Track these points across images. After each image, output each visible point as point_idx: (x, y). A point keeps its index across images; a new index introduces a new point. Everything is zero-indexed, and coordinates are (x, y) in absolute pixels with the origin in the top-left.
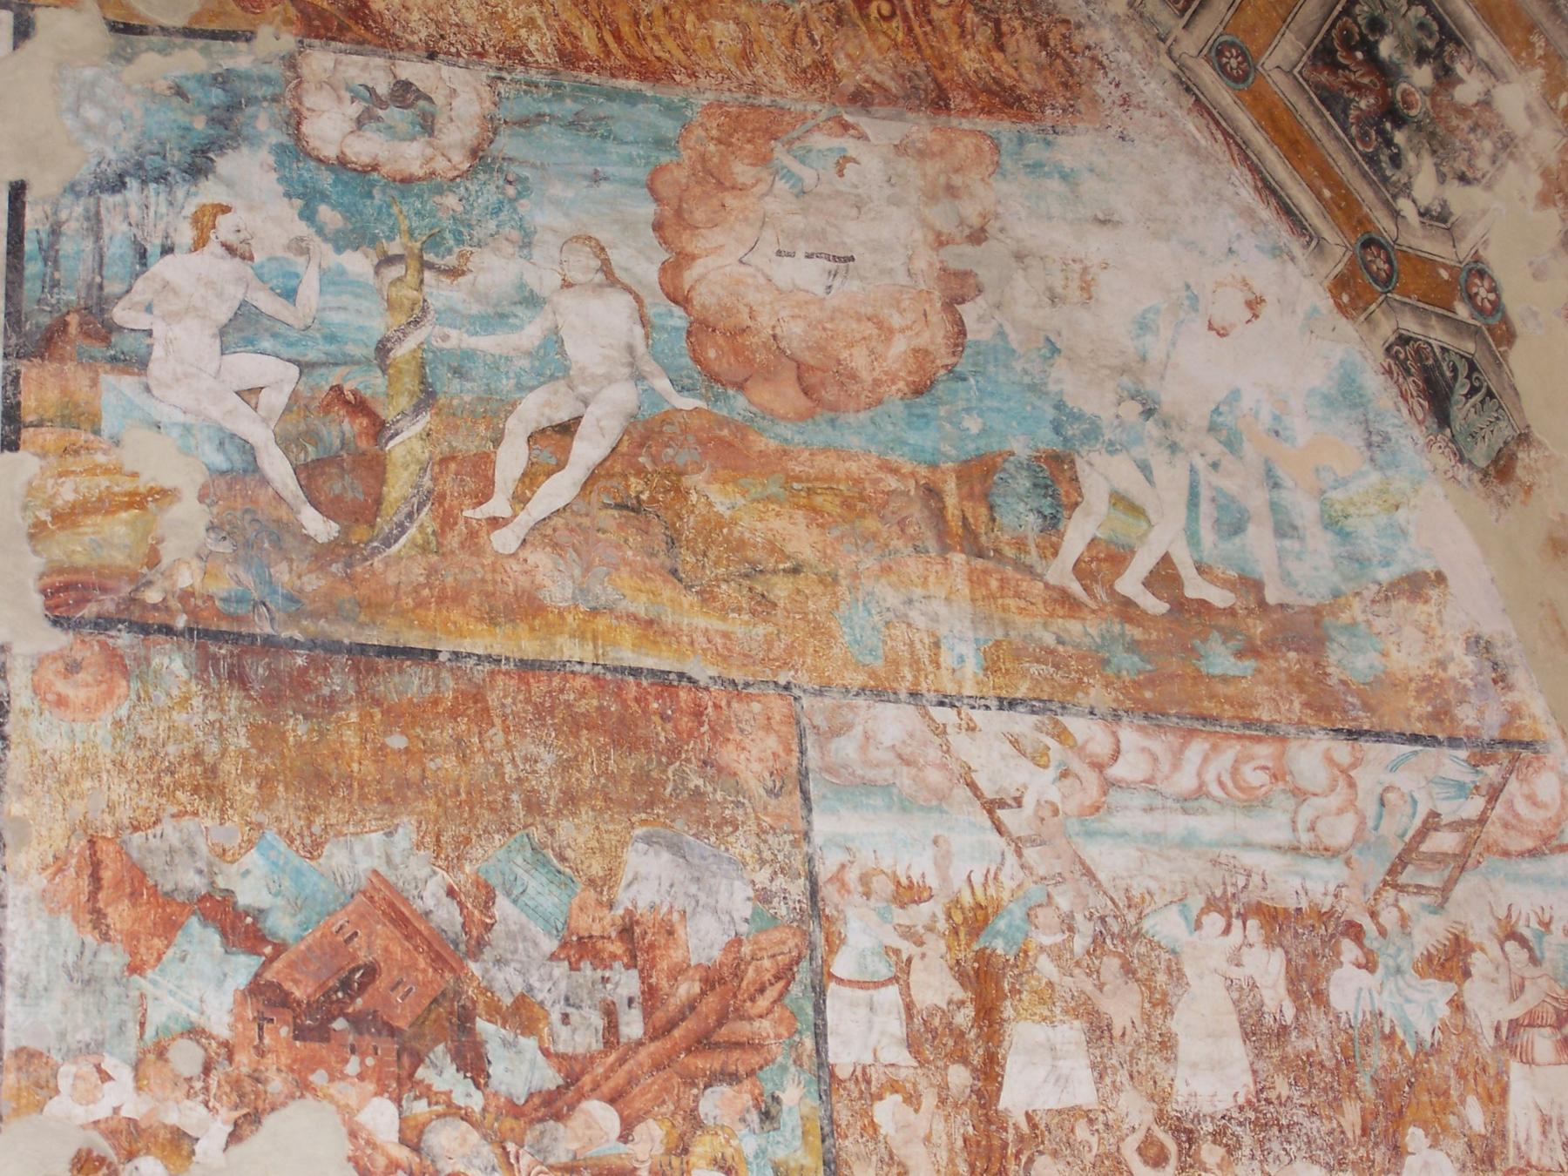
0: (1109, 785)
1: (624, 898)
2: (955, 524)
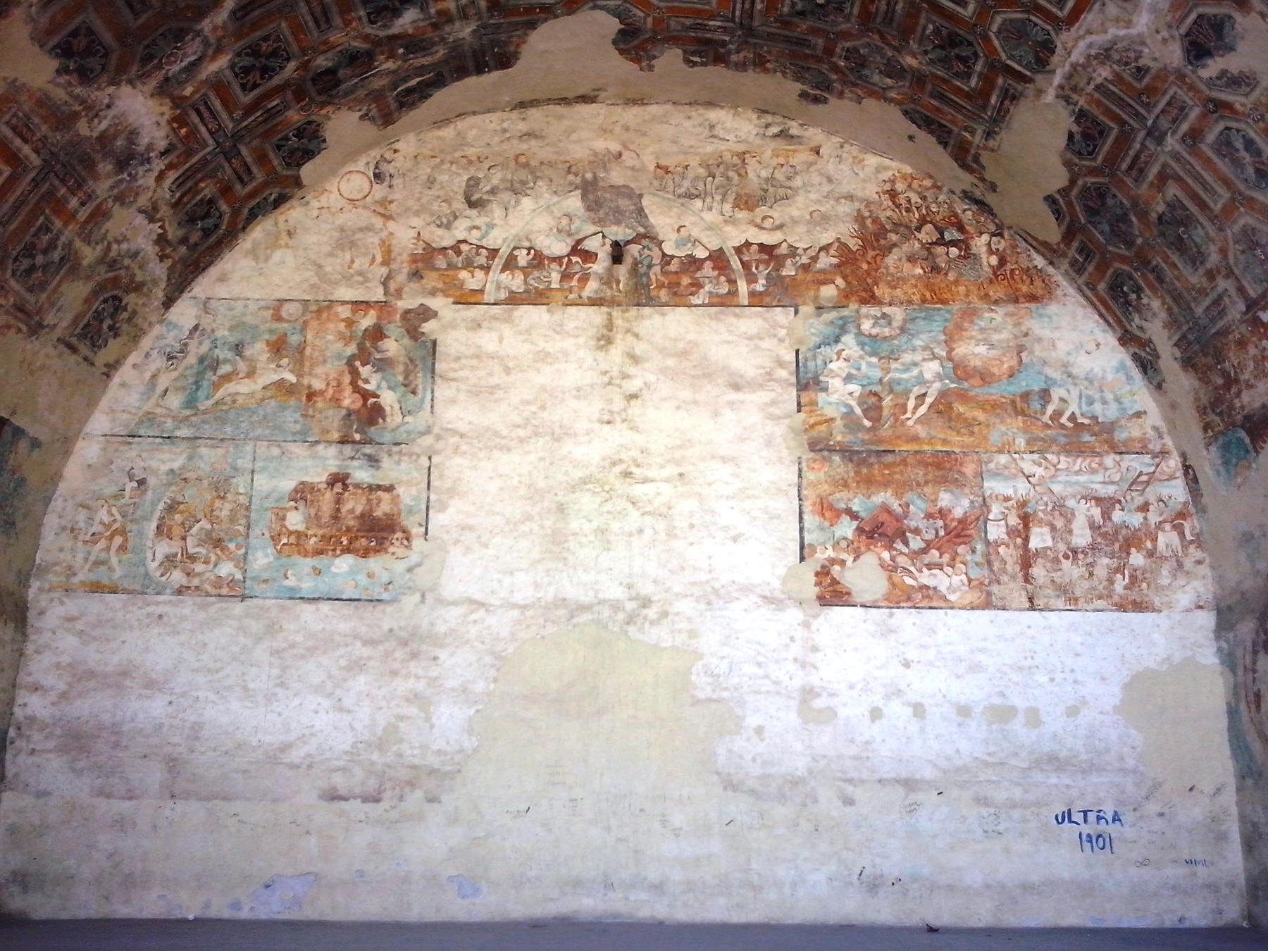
0: (1057, 470)
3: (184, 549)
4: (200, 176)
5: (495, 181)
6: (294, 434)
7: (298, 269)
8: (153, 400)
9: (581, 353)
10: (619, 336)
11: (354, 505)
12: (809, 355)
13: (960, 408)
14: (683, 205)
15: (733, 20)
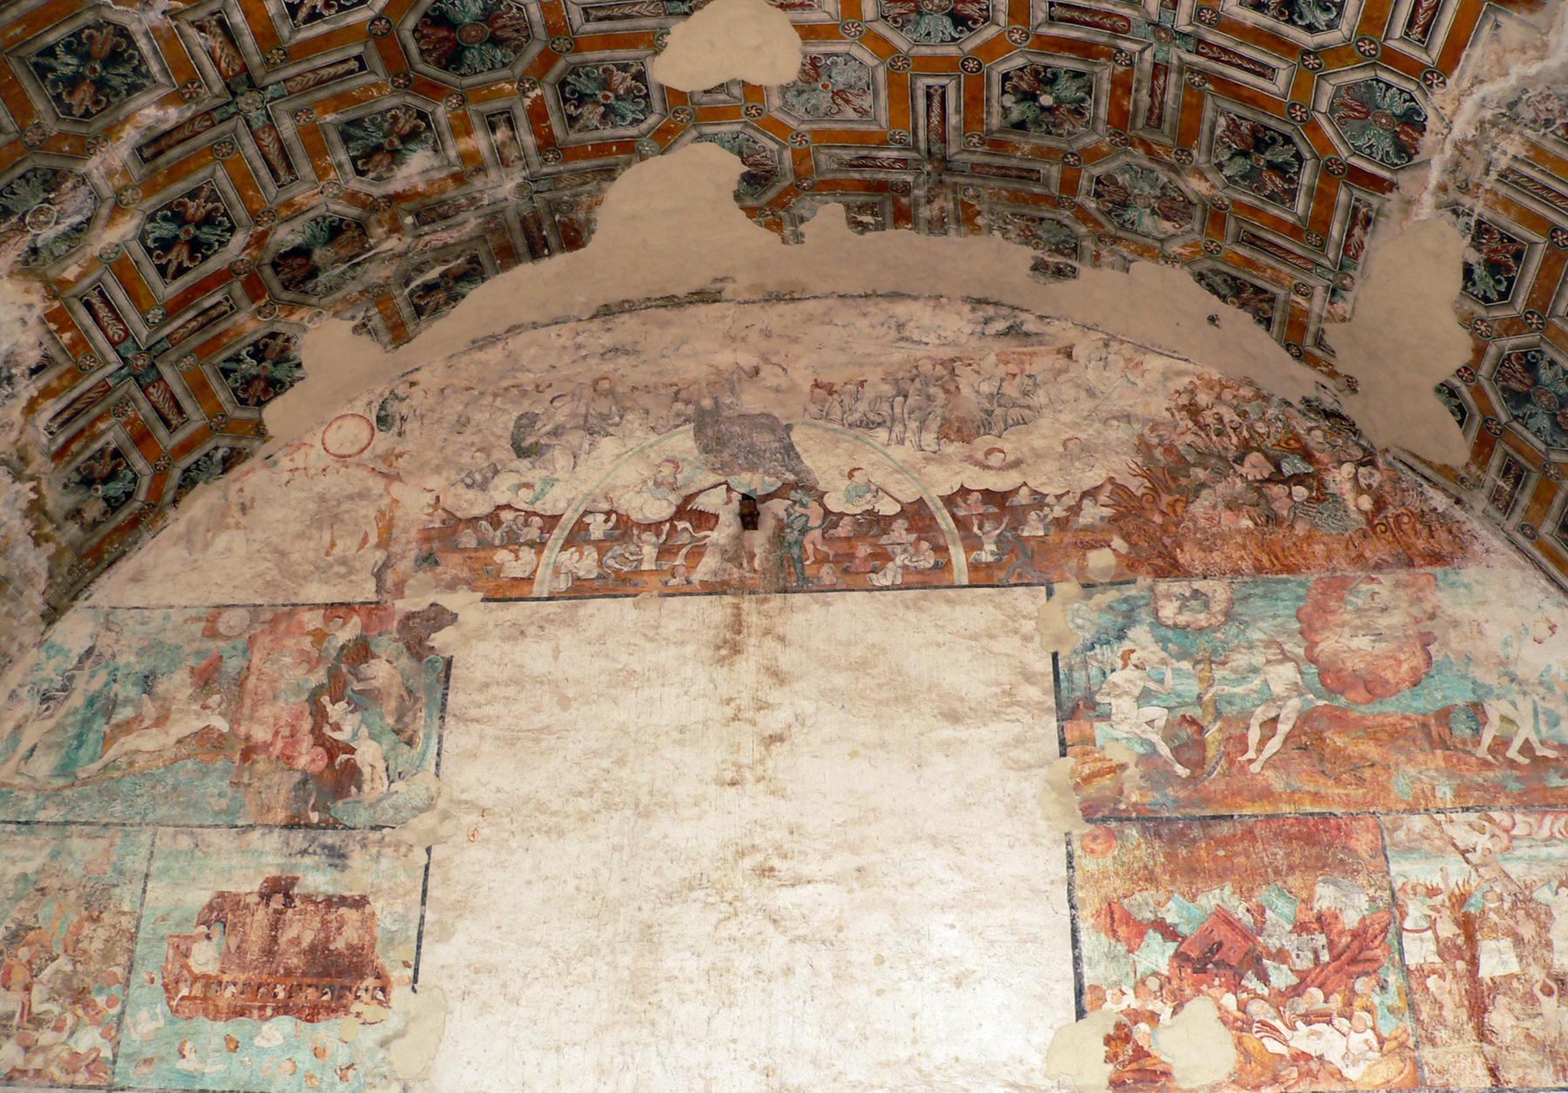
1: (1317, 906)
2: (1436, 737)
3: (26, 1007)
4: (96, 411)
5: (560, 418)
6: (217, 814)
7: (250, 559)
8: (11, 765)
9: (688, 671)
10: (753, 640)
11: (301, 930)
12: (1077, 660)
14: (857, 437)
15: (916, 148)
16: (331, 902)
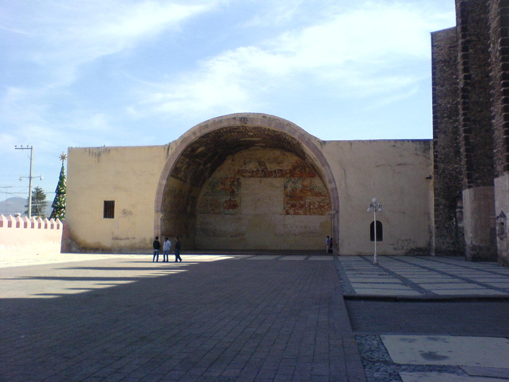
13: (303, 190)
16: (234, 201)
